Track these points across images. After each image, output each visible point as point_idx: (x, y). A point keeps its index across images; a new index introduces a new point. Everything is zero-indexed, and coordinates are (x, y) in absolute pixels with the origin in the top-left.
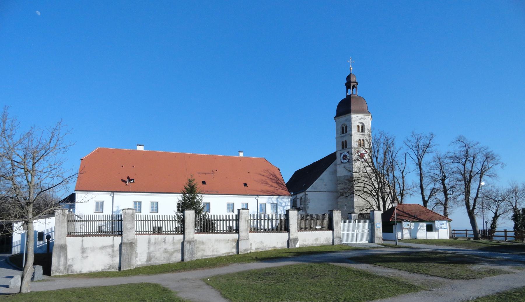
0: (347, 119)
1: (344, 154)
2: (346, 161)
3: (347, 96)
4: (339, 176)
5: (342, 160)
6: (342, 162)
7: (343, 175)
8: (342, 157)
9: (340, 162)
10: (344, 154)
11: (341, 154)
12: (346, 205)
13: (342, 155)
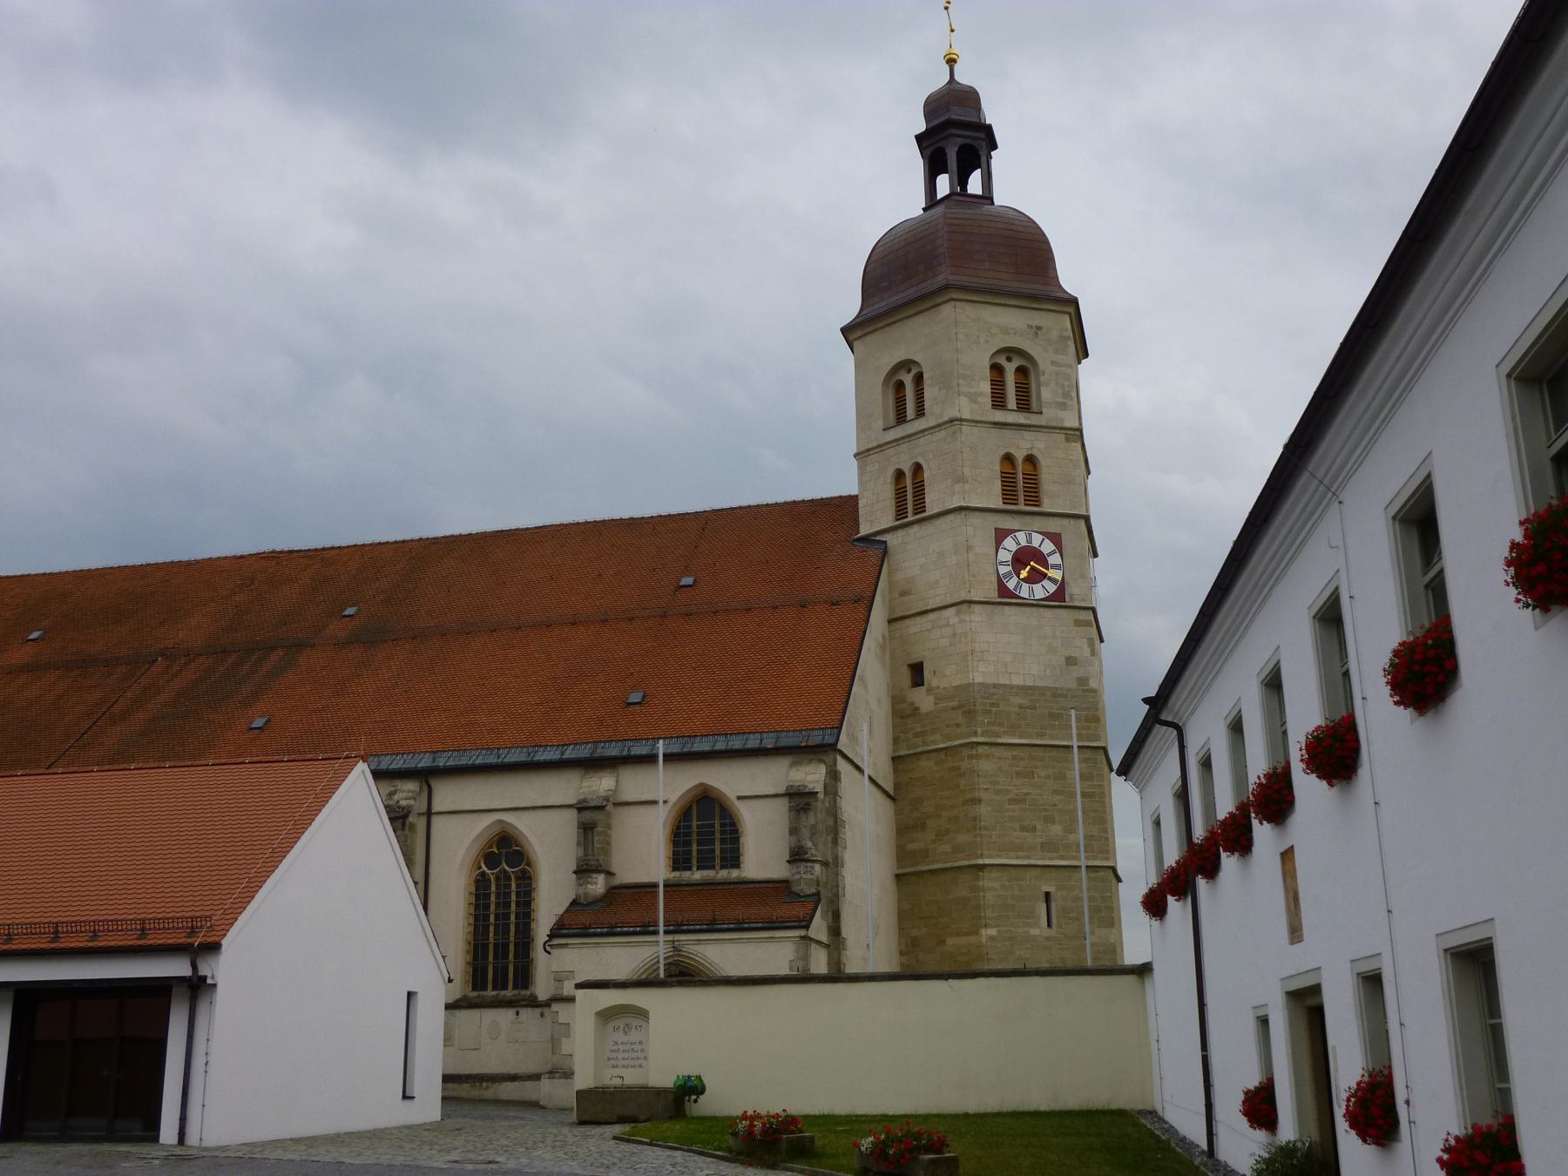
0: (1039, 328)
1: (1024, 543)
2: (1040, 591)
3: (932, 201)
4: (990, 681)
5: (1008, 575)
6: (1003, 591)
7: (1017, 681)
8: (1004, 556)
9: (993, 594)
10: (1022, 537)
11: (1001, 535)
12: (1047, 894)
13: (1010, 544)
